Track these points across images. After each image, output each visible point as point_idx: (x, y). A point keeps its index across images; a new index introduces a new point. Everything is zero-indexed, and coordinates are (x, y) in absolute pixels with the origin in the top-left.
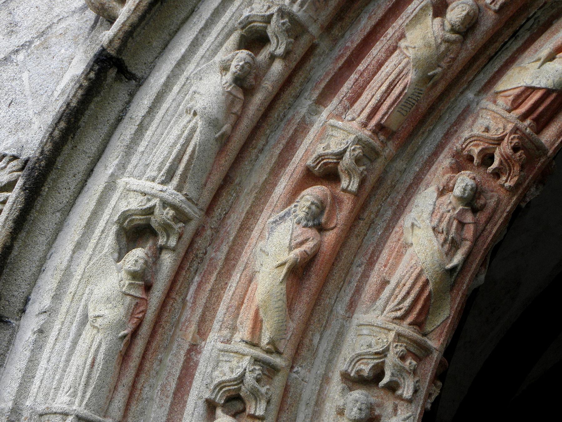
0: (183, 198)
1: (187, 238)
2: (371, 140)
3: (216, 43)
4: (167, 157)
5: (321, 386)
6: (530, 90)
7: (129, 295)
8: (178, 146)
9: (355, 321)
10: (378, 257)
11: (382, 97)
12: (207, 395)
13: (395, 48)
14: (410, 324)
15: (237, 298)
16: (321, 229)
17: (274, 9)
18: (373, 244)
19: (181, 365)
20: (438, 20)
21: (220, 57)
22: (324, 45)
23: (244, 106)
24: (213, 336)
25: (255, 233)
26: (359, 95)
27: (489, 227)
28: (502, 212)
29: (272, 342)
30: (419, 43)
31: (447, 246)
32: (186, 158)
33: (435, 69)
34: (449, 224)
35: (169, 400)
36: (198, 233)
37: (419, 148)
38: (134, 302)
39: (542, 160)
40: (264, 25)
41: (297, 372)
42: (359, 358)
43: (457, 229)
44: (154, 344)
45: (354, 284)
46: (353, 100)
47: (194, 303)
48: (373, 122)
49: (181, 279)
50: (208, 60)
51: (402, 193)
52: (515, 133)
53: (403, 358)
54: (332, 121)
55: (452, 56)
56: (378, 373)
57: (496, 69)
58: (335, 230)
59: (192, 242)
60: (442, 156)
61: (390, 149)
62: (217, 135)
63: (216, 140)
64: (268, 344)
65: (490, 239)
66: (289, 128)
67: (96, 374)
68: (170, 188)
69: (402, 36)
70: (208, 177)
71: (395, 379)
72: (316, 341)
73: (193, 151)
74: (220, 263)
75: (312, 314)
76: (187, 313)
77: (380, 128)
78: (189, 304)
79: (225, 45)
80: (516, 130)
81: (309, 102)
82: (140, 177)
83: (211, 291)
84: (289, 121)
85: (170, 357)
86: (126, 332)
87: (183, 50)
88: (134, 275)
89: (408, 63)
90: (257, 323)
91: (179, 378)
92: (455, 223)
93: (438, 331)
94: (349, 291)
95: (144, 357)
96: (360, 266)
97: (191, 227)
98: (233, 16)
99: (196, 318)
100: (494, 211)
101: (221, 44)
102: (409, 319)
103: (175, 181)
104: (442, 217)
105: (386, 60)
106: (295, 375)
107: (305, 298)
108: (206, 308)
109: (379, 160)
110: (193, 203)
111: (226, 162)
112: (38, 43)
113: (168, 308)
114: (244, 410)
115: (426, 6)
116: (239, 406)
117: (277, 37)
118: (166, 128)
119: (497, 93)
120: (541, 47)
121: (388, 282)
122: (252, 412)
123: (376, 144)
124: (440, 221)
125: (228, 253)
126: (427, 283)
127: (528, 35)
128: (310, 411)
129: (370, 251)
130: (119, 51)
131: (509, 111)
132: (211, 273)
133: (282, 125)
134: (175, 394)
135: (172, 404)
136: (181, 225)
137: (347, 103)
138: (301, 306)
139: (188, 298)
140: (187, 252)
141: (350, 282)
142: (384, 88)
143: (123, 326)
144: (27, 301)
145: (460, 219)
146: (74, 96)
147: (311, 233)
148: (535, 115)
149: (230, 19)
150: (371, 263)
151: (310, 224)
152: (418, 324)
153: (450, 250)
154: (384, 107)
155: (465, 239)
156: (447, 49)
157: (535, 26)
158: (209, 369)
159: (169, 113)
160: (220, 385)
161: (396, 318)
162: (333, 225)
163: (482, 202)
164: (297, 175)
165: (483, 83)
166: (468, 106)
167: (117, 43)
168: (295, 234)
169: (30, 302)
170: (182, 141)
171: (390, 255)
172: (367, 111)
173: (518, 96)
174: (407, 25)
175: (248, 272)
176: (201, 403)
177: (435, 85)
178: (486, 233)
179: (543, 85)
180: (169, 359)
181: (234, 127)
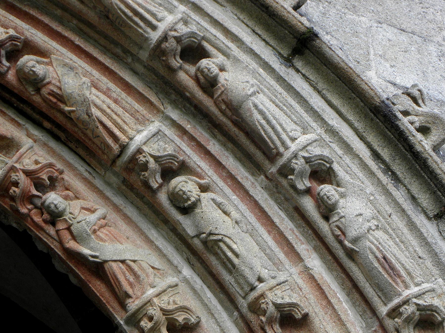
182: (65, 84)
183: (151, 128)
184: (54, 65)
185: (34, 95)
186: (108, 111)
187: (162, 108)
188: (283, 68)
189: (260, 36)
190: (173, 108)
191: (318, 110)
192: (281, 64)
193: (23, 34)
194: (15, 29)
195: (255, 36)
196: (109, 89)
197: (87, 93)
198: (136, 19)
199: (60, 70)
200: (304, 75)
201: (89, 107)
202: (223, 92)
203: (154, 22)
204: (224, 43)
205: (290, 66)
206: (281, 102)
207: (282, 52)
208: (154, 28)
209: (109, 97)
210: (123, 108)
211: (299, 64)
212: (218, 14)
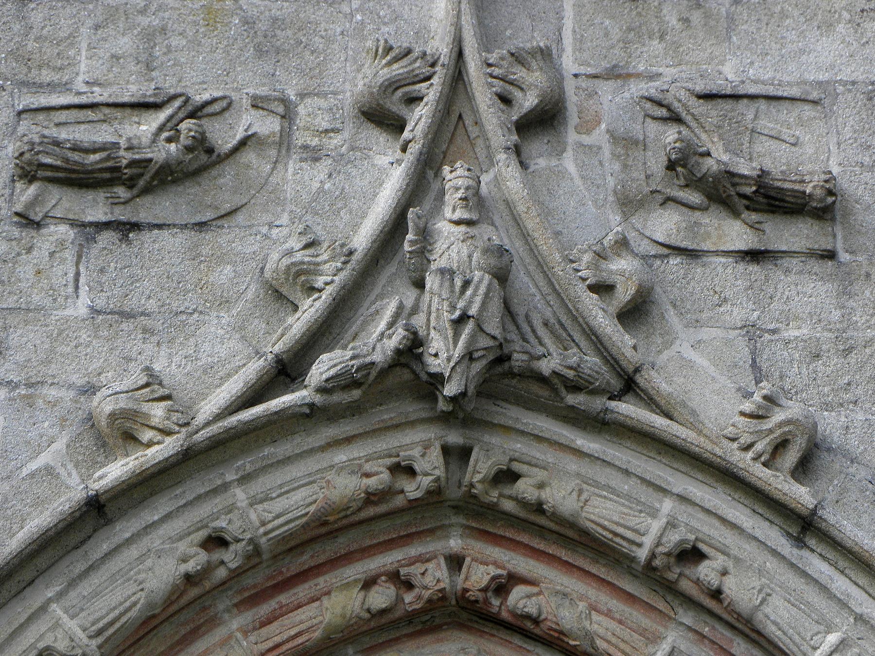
3: (186, 532)
8: (117, 612)
11: (287, 639)
13: (318, 599)
17: (248, 536)
20: (363, 593)
21: (182, 547)
22: (264, 565)
30: (338, 610)
40: (232, 541)
50: (173, 543)
66: (202, 615)
68: (94, 643)
69: (328, 593)
73: (126, 623)
79: (192, 536)
81: (228, 603)
87: (156, 518)
89: (321, 622)
98: (211, 515)
101: (189, 534)
105: (305, 605)
112: (23, 392)
115: (360, 580)
117: (236, 555)
118: (112, 585)
127: (419, 628)
130: (110, 500)
137: (258, 626)
146: (56, 525)
149: (208, 517)
157: (429, 623)
159: (121, 573)
165: (365, 647)
167: (108, 495)
170: (121, 609)
172: (270, 644)
174: (337, 587)
182: (562, 619)
183: (665, 646)
184: (546, 595)
185: (534, 628)
186: (614, 640)
187: (672, 614)
188: (795, 551)
189: (761, 515)
190: (685, 610)
191: (842, 597)
192: (792, 546)
193: (504, 568)
194: (496, 564)
195: (757, 516)
196: (610, 610)
197: (587, 624)
198: (618, 540)
199: (554, 601)
200: (821, 555)
201: (593, 641)
202: (729, 603)
203: (638, 539)
204: (720, 542)
205: (802, 547)
206: (796, 600)
207: (790, 531)
208: (640, 545)
209: (613, 618)
210: (629, 628)
211: (812, 542)
212: (709, 500)
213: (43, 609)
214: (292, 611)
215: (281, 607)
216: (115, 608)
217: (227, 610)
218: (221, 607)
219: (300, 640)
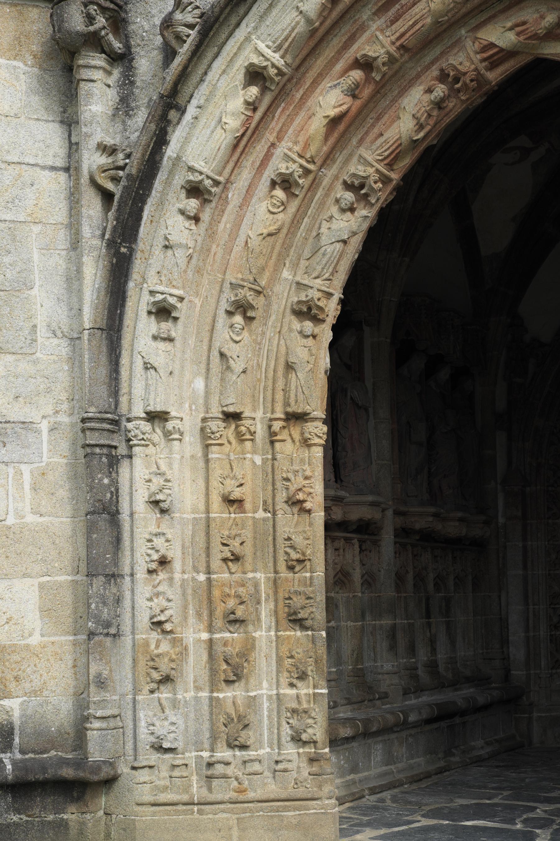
0: (283, 63)
1: (281, 84)
2: (395, 53)
4: (279, 37)
5: (333, 181)
6: (492, 45)
7: (244, 114)
9: (359, 152)
10: (383, 116)
11: (408, 28)
12: (273, 176)
14: (385, 165)
15: (300, 126)
16: (354, 97)
18: (382, 108)
19: (264, 153)
23: (331, 10)
24: (283, 143)
25: (318, 90)
26: (397, 20)
27: (445, 119)
28: (455, 112)
29: (312, 157)
31: (417, 127)
32: (290, 40)
33: (444, 17)
34: (422, 115)
35: (255, 171)
36: (289, 80)
37: (425, 56)
38: (246, 118)
39: (487, 87)
41: (322, 172)
42: (354, 175)
43: (426, 118)
44: (253, 139)
45: (365, 129)
46: (393, 22)
47: (278, 119)
48: (398, 44)
49: (274, 105)
51: (407, 82)
52: (475, 71)
53: (375, 182)
54: (378, 33)
55: (456, 11)
56: (362, 186)
57: (482, 20)
58: (362, 100)
59: (285, 85)
60: (434, 67)
61: (406, 57)
62: (310, 29)
63: (310, 31)
64: (309, 158)
65: (444, 125)
66: (354, 25)
67: (220, 154)
70: (301, 51)
71: (369, 192)
72: (337, 156)
73: (295, 37)
74: (297, 100)
75: (338, 142)
76: (273, 124)
77: (402, 47)
78: (276, 119)
80: (476, 69)
82: (263, 42)
83: (289, 115)
84: (356, 21)
85: (260, 146)
86: (238, 135)
88: (247, 103)
90: (307, 145)
91: (262, 161)
92: (426, 115)
93: (400, 169)
94: (362, 131)
95: (246, 146)
96: (371, 119)
97: (286, 78)
99: (277, 129)
100: (451, 110)
102: (385, 162)
103: (282, 52)
104: (420, 109)
106: (321, 173)
107: (336, 135)
108: (284, 125)
109: (397, 64)
110: (289, 66)
111: (312, 44)
113: (264, 120)
114: (290, 188)
116: (287, 185)
119: (477, 38)
120: (511, 16)
121: (382, 135)
122: (293, 191)
123: (397, 55)
124: (418, 112)
125: (303, 95)
126: (401, 144)
128: (324, 193)
129: (379, 112)
131: (478, 53)
132: (291, 105)
133: (351, 22)
134: (258, 169)
135: (255, 174)
136: (279, 78)
137: (389, 24)
138: (332, 139)
139: (276, 115)
140: (281, 90)
141: (364, 127)
142: (411, 23)
143: (238, 131)
144: (192, 96)
145: (429, 112)
147: (349, 100)
148: (491, 60)
150: (378, 119)
151: (349, 94)
152: (390, 166)
153: (418, 129)
154: (408, 35)
155: (429, 124)
156: (454, 7)
158: (277, 162)
160: (281, 174)
161: (379, 160)
162: (361, 97)
163: (445, 105)
164: (350, 61)
166: (460, 38)
168: (339, 99)
169: (193, 97)
171: (388, 119)
172: (398, 34)
173: (485, 46)
175: (310, 112)
176: (269, 180)
177: (441, 25)
178: (442, 122)
179: (500, 45)
180: (258, 148)
181: (321, 24)
213: (248, 39)
214: (410, 8)
215: (402, 7)
216: (286, 29)
217: (371, 19)
218: (365, 17)
219: (417, 27)
